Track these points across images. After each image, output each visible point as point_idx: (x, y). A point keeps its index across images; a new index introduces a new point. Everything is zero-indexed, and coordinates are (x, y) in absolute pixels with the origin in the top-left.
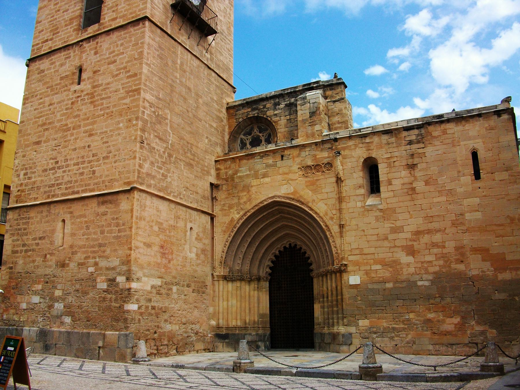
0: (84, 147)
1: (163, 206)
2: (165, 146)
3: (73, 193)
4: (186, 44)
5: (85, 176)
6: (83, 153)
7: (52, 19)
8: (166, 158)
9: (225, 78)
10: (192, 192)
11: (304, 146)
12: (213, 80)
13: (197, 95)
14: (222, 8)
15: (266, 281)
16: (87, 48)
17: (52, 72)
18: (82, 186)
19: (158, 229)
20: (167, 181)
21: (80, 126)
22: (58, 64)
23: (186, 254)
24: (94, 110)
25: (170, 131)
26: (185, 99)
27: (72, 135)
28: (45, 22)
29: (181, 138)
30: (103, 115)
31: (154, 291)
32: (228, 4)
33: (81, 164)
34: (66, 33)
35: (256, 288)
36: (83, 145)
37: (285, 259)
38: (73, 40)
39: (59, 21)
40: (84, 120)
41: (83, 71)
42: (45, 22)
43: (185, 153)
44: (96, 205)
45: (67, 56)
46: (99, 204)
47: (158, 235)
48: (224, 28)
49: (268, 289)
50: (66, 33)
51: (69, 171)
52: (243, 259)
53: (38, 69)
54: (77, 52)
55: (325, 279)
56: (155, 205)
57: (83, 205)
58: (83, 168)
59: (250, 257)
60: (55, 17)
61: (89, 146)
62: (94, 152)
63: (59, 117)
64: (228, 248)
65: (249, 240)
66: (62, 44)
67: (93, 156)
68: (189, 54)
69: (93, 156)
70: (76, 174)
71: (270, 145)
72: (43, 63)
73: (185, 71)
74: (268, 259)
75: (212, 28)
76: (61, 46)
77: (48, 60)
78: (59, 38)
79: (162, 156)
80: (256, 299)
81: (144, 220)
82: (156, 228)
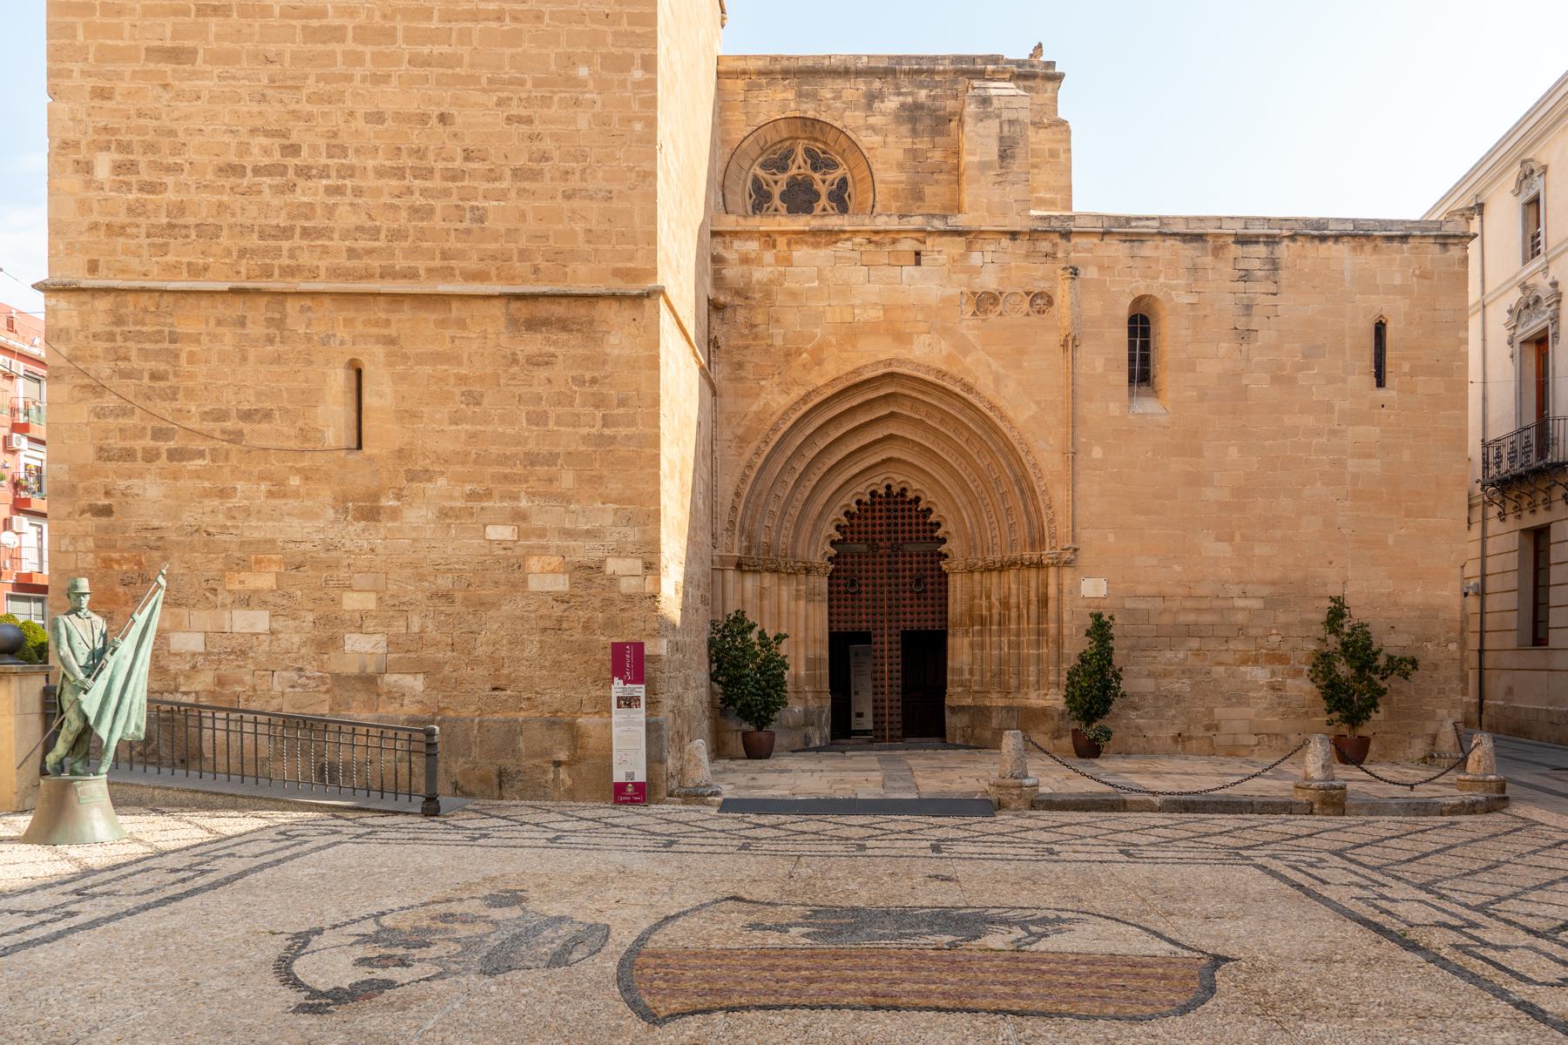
0: (423, 119)
5: (437, 222)
6: (416, 137)
30: (499, 19)
33: (415, 177)
36: (413, 108)
44: (503, 330)
46: (513, 322)
57: (442, 324)
62: (468, 143)
67: (467, 159)
69: (467, 159)
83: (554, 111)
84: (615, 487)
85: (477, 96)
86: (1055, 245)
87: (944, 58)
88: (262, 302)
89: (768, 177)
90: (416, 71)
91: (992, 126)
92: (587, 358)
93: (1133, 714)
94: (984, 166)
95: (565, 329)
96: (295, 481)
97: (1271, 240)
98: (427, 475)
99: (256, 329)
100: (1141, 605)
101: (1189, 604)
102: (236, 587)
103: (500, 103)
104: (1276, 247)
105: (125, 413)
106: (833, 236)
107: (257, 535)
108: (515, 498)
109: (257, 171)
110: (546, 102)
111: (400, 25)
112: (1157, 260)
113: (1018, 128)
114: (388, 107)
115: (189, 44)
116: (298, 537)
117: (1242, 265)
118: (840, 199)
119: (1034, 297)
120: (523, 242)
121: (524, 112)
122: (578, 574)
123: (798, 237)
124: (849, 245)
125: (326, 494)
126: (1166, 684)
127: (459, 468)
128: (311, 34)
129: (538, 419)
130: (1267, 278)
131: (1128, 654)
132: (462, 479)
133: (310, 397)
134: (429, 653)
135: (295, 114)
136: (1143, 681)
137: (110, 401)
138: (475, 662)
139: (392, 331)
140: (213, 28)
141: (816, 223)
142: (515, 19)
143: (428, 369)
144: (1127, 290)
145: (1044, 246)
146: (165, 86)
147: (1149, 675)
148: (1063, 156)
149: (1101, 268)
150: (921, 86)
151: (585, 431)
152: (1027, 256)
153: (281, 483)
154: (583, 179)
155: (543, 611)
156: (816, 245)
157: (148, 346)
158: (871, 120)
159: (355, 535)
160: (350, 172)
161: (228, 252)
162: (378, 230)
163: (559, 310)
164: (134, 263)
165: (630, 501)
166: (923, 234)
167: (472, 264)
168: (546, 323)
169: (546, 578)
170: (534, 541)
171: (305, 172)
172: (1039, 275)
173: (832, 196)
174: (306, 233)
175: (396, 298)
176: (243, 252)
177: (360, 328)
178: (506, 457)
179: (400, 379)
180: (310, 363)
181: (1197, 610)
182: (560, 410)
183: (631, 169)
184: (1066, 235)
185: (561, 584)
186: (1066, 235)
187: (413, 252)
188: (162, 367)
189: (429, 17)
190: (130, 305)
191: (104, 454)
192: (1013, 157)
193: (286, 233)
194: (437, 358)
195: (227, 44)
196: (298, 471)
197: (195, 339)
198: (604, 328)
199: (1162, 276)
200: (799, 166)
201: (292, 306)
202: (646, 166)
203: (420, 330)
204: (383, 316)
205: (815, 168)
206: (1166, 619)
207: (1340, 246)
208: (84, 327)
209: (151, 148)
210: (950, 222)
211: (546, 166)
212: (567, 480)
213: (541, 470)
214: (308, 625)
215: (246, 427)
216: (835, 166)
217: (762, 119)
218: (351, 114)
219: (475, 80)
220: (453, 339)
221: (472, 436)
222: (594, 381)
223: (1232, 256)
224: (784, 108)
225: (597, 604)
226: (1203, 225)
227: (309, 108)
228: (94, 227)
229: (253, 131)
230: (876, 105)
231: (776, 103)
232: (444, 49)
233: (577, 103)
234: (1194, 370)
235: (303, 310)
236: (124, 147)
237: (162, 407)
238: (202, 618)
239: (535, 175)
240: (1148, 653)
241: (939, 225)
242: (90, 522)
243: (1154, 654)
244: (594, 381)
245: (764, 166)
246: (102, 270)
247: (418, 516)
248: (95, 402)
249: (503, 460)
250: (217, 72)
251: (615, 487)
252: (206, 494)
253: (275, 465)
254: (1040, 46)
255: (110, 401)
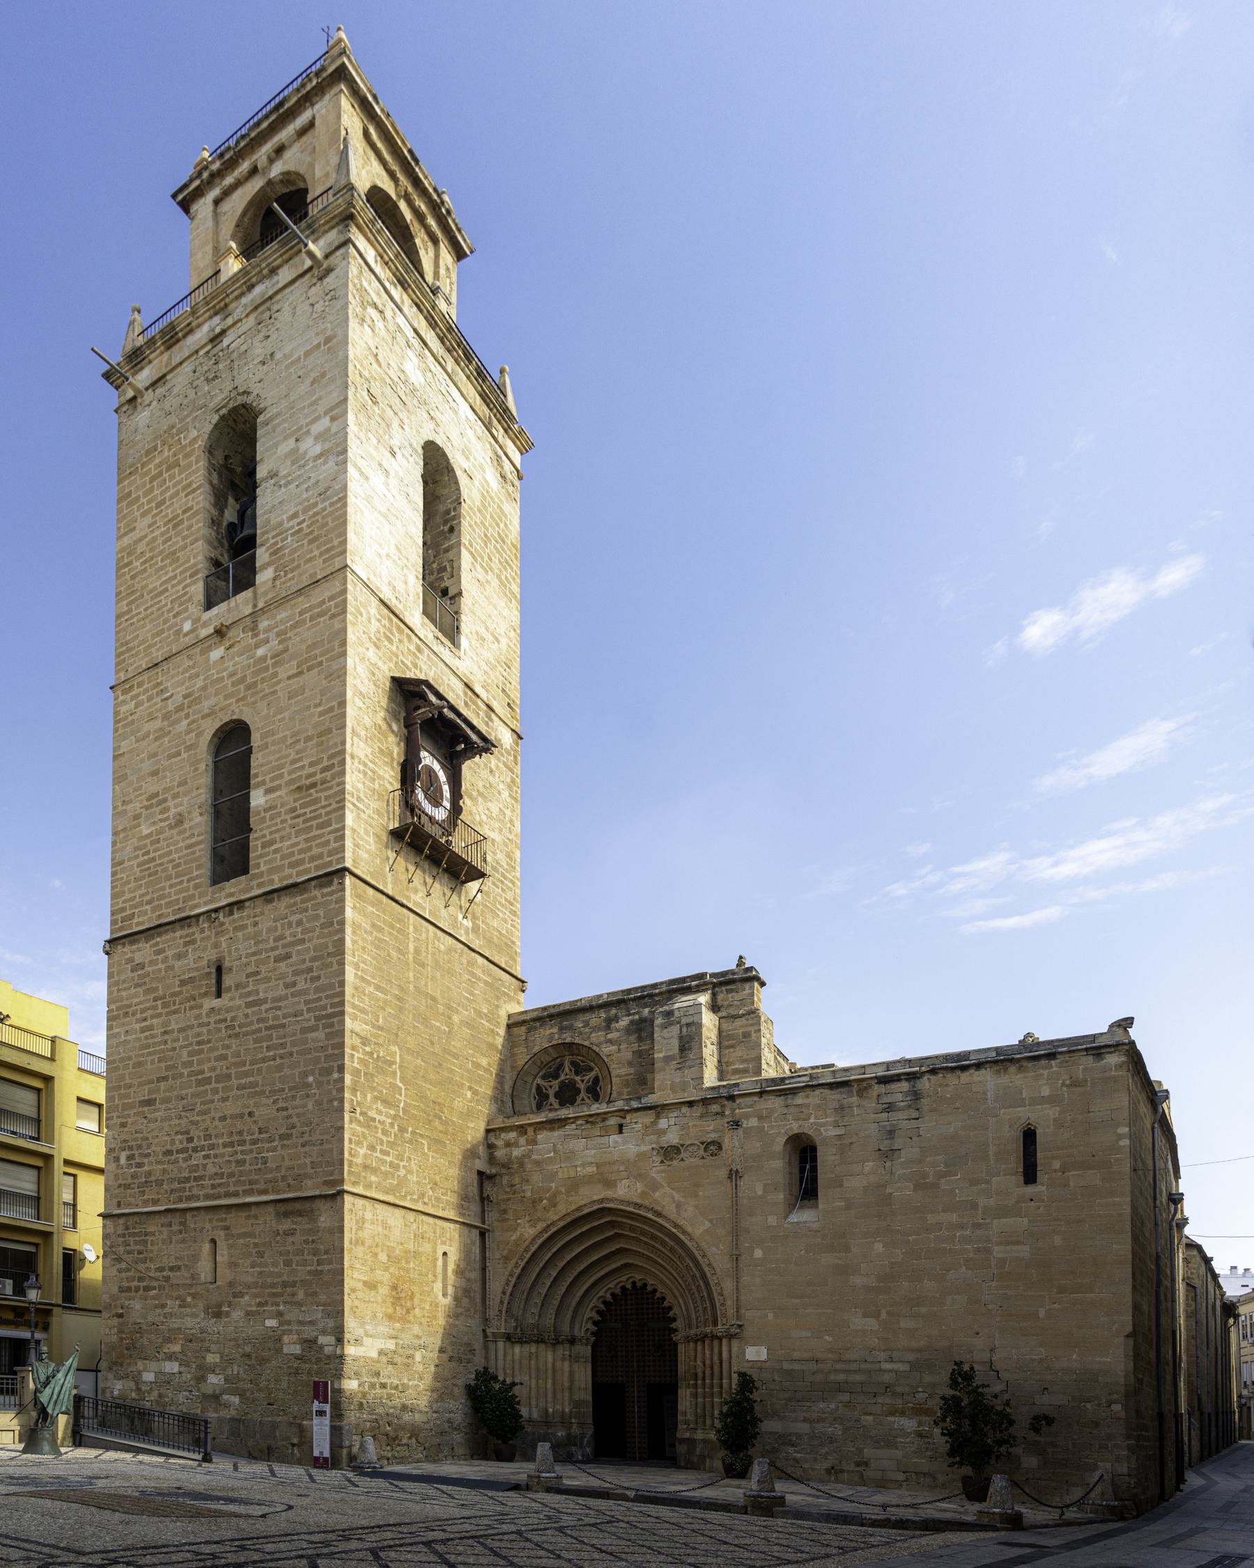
1: (395, 1218)
2: (392, 1112)
3: (227, 1195)
4: (424, 909)
5: (247, 1167)
6: (239, 1126)
7: (146, 857)
8: (395, 1135)
9: (503, 965)
10: (444, 1191)
11: (664, 1107)
12: (479, 973)
13: (450, 1008)
14: (495, 811)
16: (227, 924)
17: (160, 970)
18: (243, 1183)
19: (386, 1258)
20: (399, 1176)
21: (228, 1077)
22: (170, 953)
23: (436, 1297)
24: (255, 1048)
25: (401, 1085)
26: (425, 1021)
27: (215, 1091)
28: (131, 863)
29: (423, 1097)
31: (384, 1359)
32: (509, 799)
34: (181, 891)
36: (238, 1111)
38: (196, 906)
39: (161, 865)
40: (236, 1065)
41: (224, 971)
42: (131, 863)
43: (430, 1121)
45: (188, 939)
46: (278, 1214)
47: (386, 1269)
48: (500, 856)
50: (181, 891)
51: (216, 1156)
52: (542, 1305)
53: (131, 960)
54: (207, 933)
55: (699, 1347)
56: (380, 1218)
57: (248, 1218)
58: (242, 1152)
59: (556, 1303)
60: (152, 855)
61: (251, 1114)
62: (260, 1124)
63: (185, 1058)
64: (514, 1286)
65: (554, 1274)
66: (174, 913)
67: (260, 1133)
68: (431, 927)
69: (260, 1133)
70: (229, 1162)
71: (596, 1106)
72: (139, 950)
73: (423, 965)
75: (476, 868)
76: (172, 918)
77: (148, 945)
78: (167, 900)
79: (387, 1131)
80: (566, 1375)
81: (363, 1244)
82: (383, 1257)
83: (298, 1102)
84: (322, 1298)
85: (264, 1101)
86: (723, 1106)
87: (662, 983)
88: (178, 1214)
89: (545, 1084)
90: (239, 1093)
91: (675, 1030)
92: (310, 1230)
93: (791, 1450)
94: (667, 1059)
95: (300, 1215)
96: (189, 1299)
97: (912, 1077)
98: (241, 1295)
99: (175, 1228)
100: (797, 1367)
101: (839, 1366)
102: (166, 1351)
103: (275, 1102)
104: (917, 1081)
105: (129, 1270)
106: (563, 1122)
107: (175, 1326)
108: (278, 1305)
109: (178, 1152)
110: (294, 1098)
111: (233, 1071)
112: (808, 1106)
113: (694, 1029)
114: (228, 1113)
115: (154, 1096)
116: (190, 1326)
117: (886, 1100)
118: (594, 1092)
119: (707, 1145)
120: (283, 1172)
121: (285, 1105)
122: (305, 1345)
123: (539, 1126)
124: (574, 1126)
125: (201, 1305)
126: (819, 1428)
127: (254, 1290)
128: (200, 1083)
129: (288, 1263)
130: (909, 1107)
131: (786, 1405)
132: (255, 1296)
133: (195, 1258)
134: (241, 1385)
135: (192, 1122)
136: (800, 1425)
137: (124, 1265)
138: (260, 1390)
139: (227, 1223)
140: (162, 1087)
141: (551, 1115)
142: (281, 1058)
143: (242, 1241)
144: (783, 1131)
145: (715, 1108)
146: (145, 1117)
147: (805, 1420)
148: (754, 1035)
149: (761, 1118)
150: (645, 1006)
151: (309, 1268)
152: (702, 1117)
153: (184, 1300)
154: (310, 1135)
155: (290, 1364)
156: (552, 1129)
157: (137, 1239)
158: (609, 1036)
159: (212, 1326)
160: (212, 1147)
161: (166, 1191)
162: (223, 1174)
163: (298, 1206)
164: (132, 1200)
165: (330, 1305)
166: (623, 1113)
167: (261, 1186)
168: (292, 1213)
169: (291, 1347)
170: (286, 1327)
171: (195, 1150)
172: (710, 1128)
173: (588, 1090)
174: (196, 1179)
175: (229, 1207)
176: (172, 1191)
177: (215, 1223)
178: (275, 1284)
179: (230, 1247)
180: (196, 1241)
181: (848, 1372)
182: (298, 1258)
183: (332, 1127)
184: (732, 1098)
185: (297, 1350)
186: (732, 1098)
187: (238, 1183)
188: (142, 1248)
189: (245, 1065)
190: (131, 1220)
191: (121, 1290)
192: (690, 1049)
193: (187, 1180)
194: (246, 1235)
195: (167, 1094)
196: (190, 1294)
197: (153, 1234)
198: (318, 1213)
199: (813, 1117)
200: (567, 1074)
201: (189, 1215)
202: (339, 1124)
203: (239, 1222)
204: (224, 1216)
205: (577, 1074)
206: (819, 1378)
207: (983, 1072)
208: (115, 1232)
209: (140, 1147)
210: (643, 1101)
211: (294, 1131)
212: (301, 1295)
213: (289, 1290)
214: (193, 1370)
215: (171, 1274)
216: (591, 1069)
217: (537, 1049)
218: (213, 1119)
219: (263, 1092)
220: (252, 1225)
221: (260, 1273)
222: (313, 1241)
223: (875, 1094)
224: (551, 1037)
225: (314, 1360)
226: (849, 1074)
227: (197, 1118)
228: (120, 1186)
229: (177, 1133)
230: (613, 1025)
231: (546, 1037)
232: (252, 1079)
233: (308, 1096)
234: (841, 1186)
235: (194, 1216)
236: (130, 1148)
237: (141, 1267)
238: (153, 1365)
239: (289, 1136)
240: (803, 1403)
241: (635, 1104)
242: (116, 1321)
243: (808, 1404)
244: (313, 1241)
245: (543, 1078)
246: (122, 1205)
247: (237, 1315)
248: (118, 1266)
249: (273, 1285)
250: (164, 1107)
251: (322, 1298)
252: (156, 1307)
253: (182, 1292)
254: (741, 957)
255: (124, 1265)
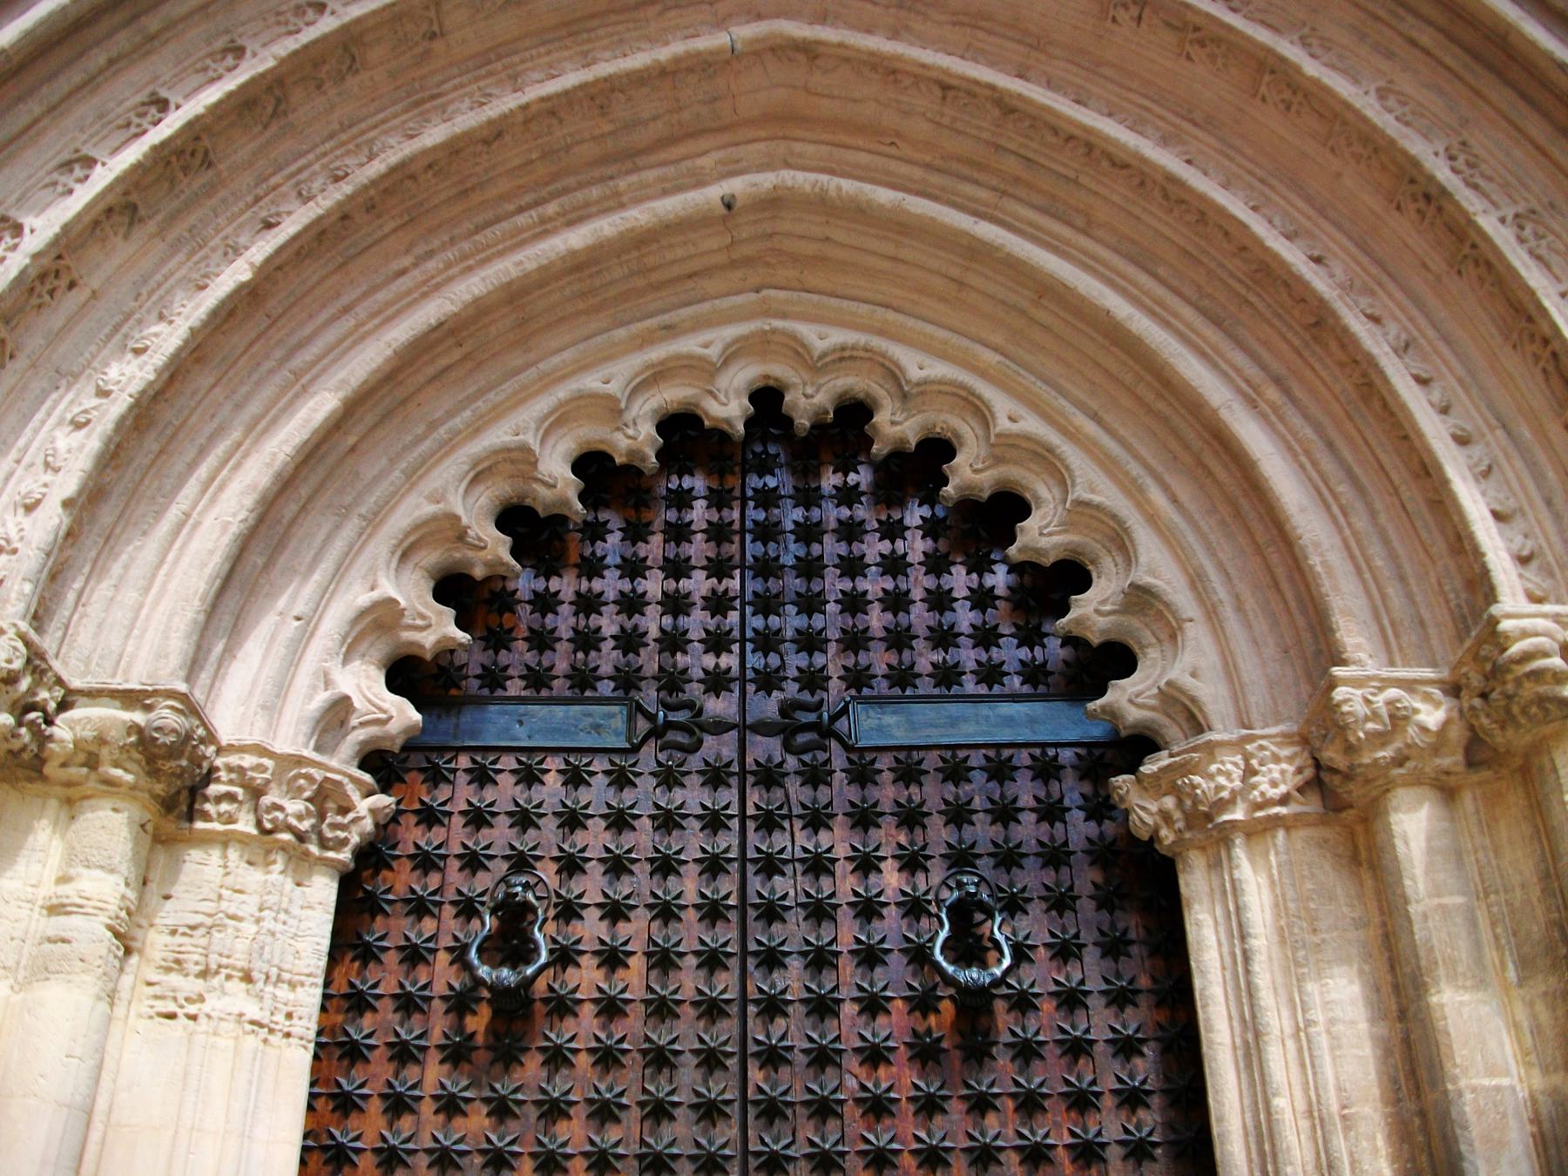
15: (300, 863)
35: (91, 933)
37: (653, 585)
49: (310, 998)
74: (403, 518)
